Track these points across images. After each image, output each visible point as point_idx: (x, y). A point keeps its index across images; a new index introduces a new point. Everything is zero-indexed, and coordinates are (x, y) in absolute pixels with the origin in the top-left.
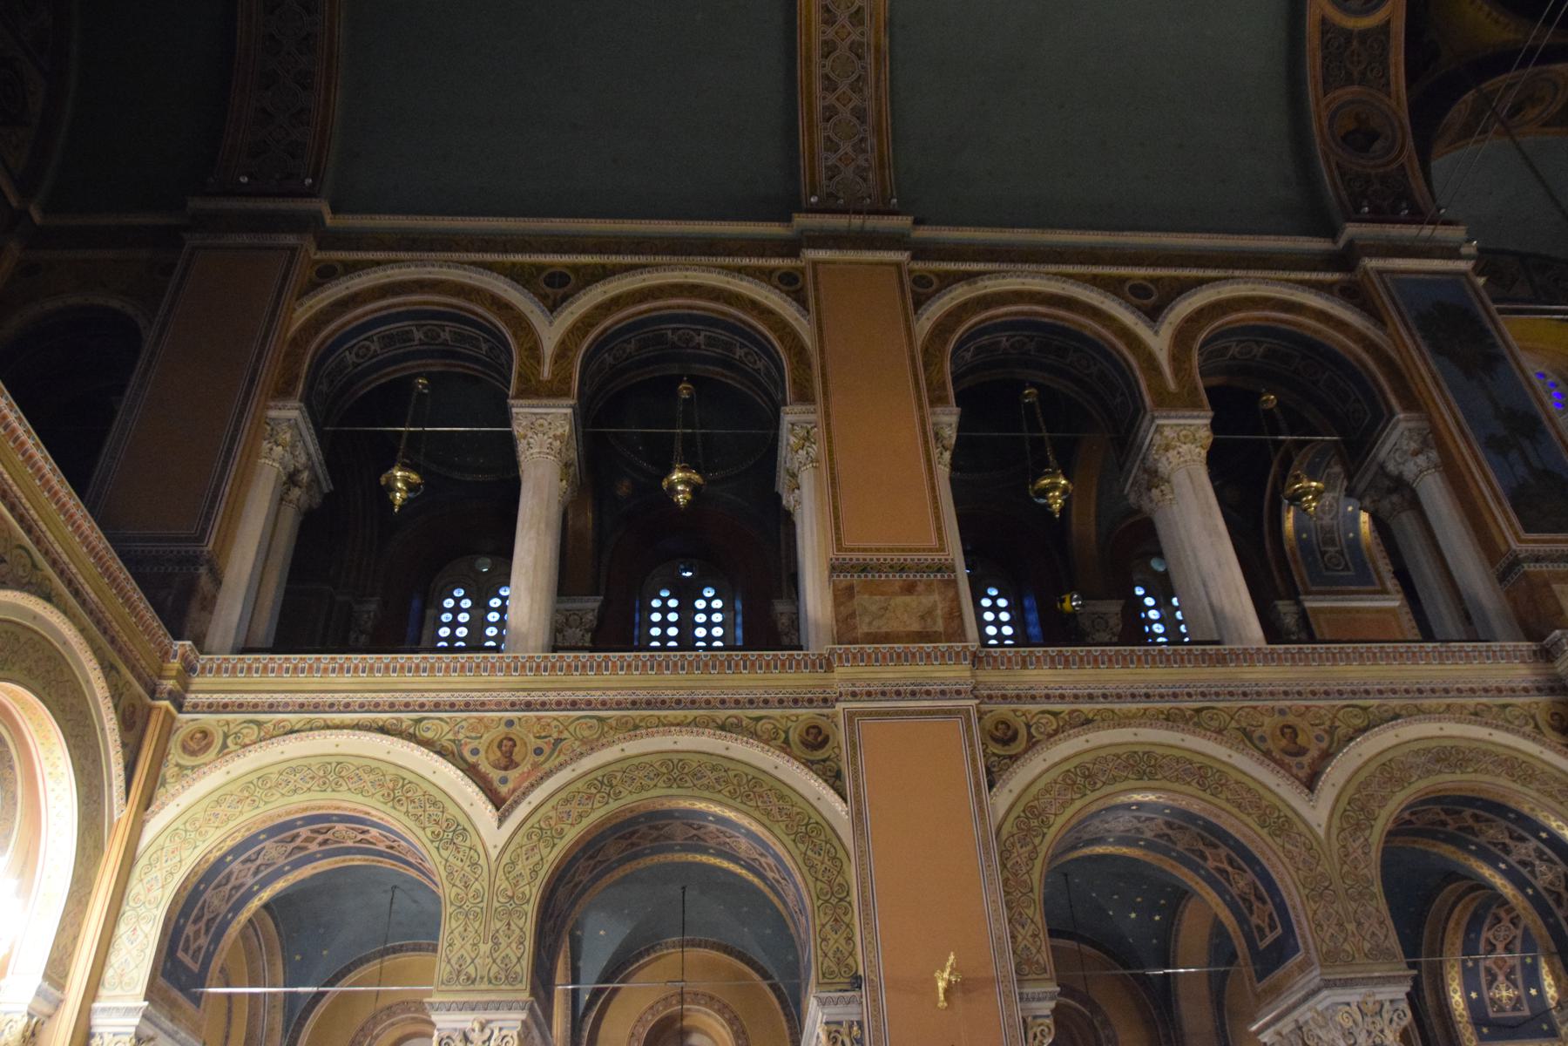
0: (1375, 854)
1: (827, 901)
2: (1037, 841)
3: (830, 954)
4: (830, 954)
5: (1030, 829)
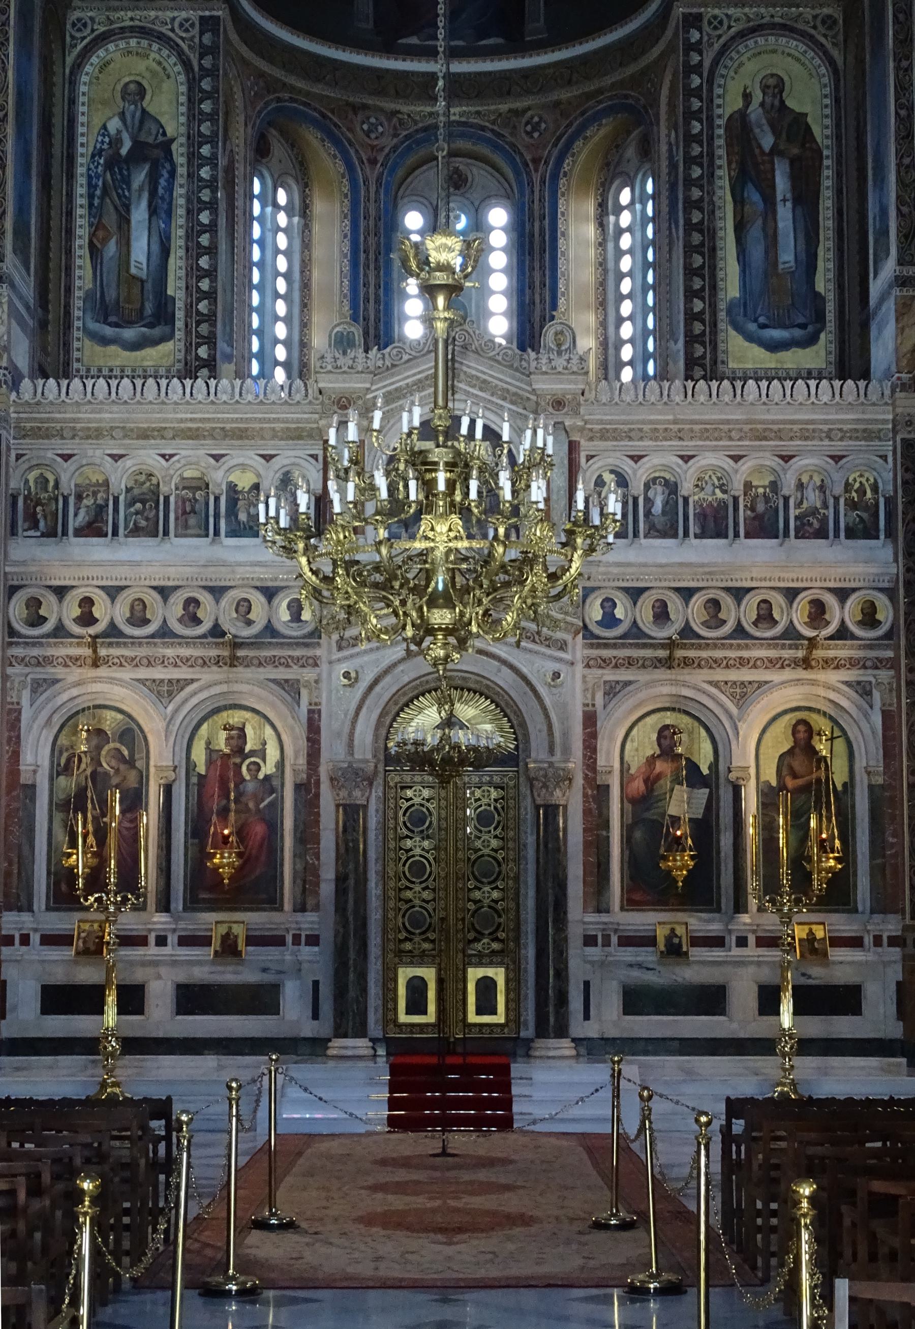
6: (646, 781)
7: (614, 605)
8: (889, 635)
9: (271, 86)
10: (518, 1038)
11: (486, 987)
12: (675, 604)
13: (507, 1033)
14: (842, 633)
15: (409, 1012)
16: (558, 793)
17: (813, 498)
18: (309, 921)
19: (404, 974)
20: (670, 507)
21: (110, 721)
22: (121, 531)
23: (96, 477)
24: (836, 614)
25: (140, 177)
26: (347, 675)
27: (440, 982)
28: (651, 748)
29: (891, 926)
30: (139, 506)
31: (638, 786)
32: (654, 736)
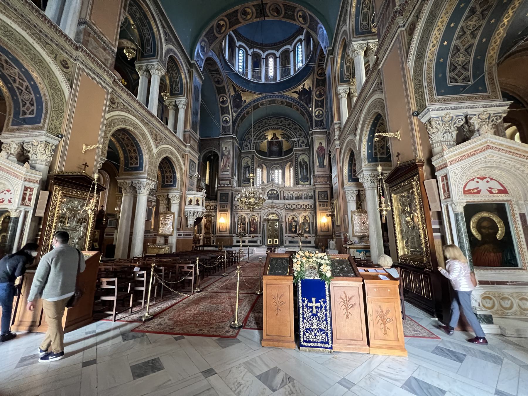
0: (159, 162)
1: (56, 111)
2: (112, 128)
3: (53, 125)
4: (53, 125)
5: (111, 125)
9: (259, 161)
11: (276, 241)
12: (293, 205)
14: (309, 208)
17: (306, 196)
18: (260, 235)
19: (269, 240)
20: (292, 197)
21: (243, 217)
24: (308, 206)
25: (247, 169)
29: (314, 235)
31: (290, 222)
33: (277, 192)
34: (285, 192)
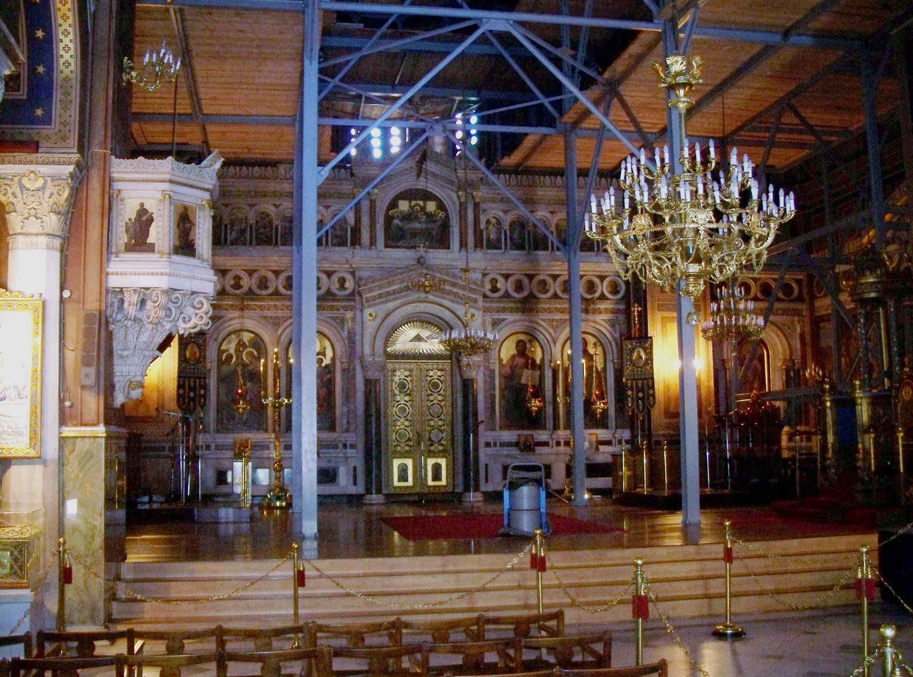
6: (511, 367)
7: (497, 282)
8: (623, 298)
10: (453, 492)
11: (437, 468)
13: (450, 489)
15: (399, 481)
16: (474, 373)
18: (350, 438)
19: (396, 463)
21: (247, 337)
22: (254, 241)
23: (240, 216)
26: (371, 315)
27: (414, 467)
28: (513, 351)
30: (262, 230)
31: (507, 370)
32: (514, 345)
33: (441, 206)
34: (483, 206)
